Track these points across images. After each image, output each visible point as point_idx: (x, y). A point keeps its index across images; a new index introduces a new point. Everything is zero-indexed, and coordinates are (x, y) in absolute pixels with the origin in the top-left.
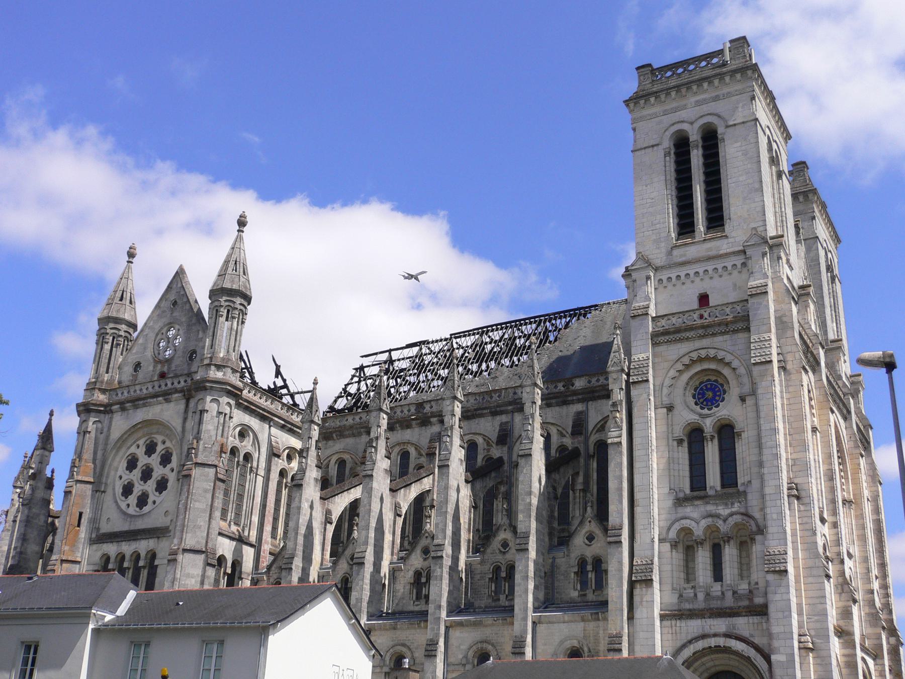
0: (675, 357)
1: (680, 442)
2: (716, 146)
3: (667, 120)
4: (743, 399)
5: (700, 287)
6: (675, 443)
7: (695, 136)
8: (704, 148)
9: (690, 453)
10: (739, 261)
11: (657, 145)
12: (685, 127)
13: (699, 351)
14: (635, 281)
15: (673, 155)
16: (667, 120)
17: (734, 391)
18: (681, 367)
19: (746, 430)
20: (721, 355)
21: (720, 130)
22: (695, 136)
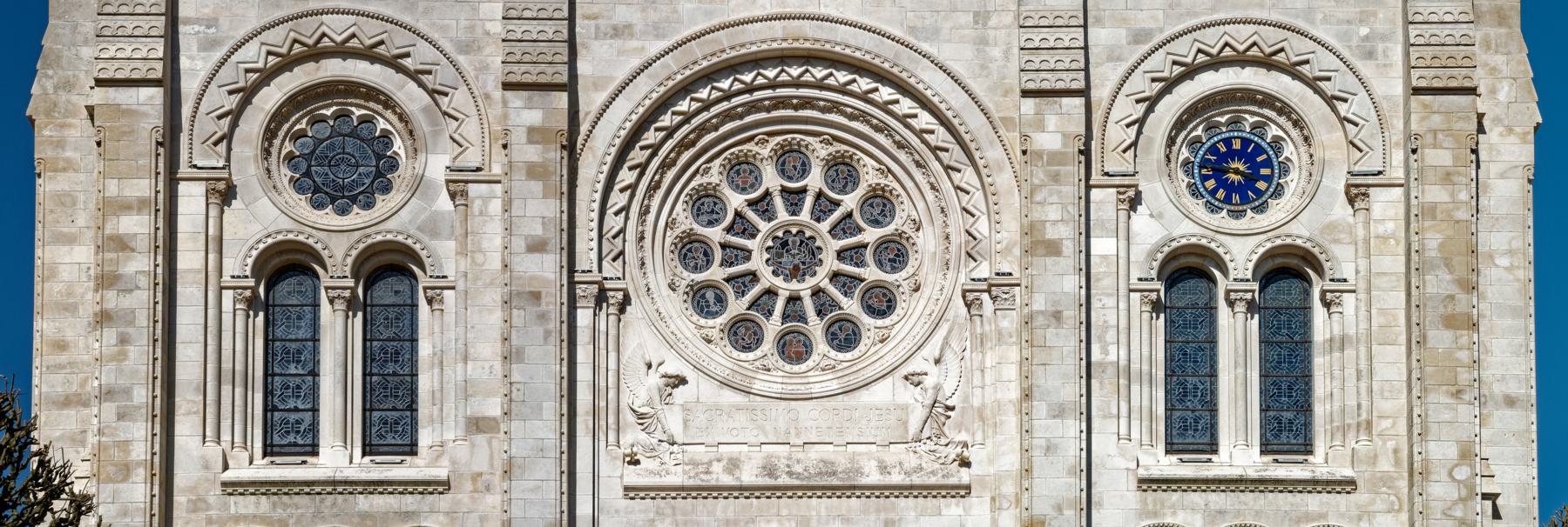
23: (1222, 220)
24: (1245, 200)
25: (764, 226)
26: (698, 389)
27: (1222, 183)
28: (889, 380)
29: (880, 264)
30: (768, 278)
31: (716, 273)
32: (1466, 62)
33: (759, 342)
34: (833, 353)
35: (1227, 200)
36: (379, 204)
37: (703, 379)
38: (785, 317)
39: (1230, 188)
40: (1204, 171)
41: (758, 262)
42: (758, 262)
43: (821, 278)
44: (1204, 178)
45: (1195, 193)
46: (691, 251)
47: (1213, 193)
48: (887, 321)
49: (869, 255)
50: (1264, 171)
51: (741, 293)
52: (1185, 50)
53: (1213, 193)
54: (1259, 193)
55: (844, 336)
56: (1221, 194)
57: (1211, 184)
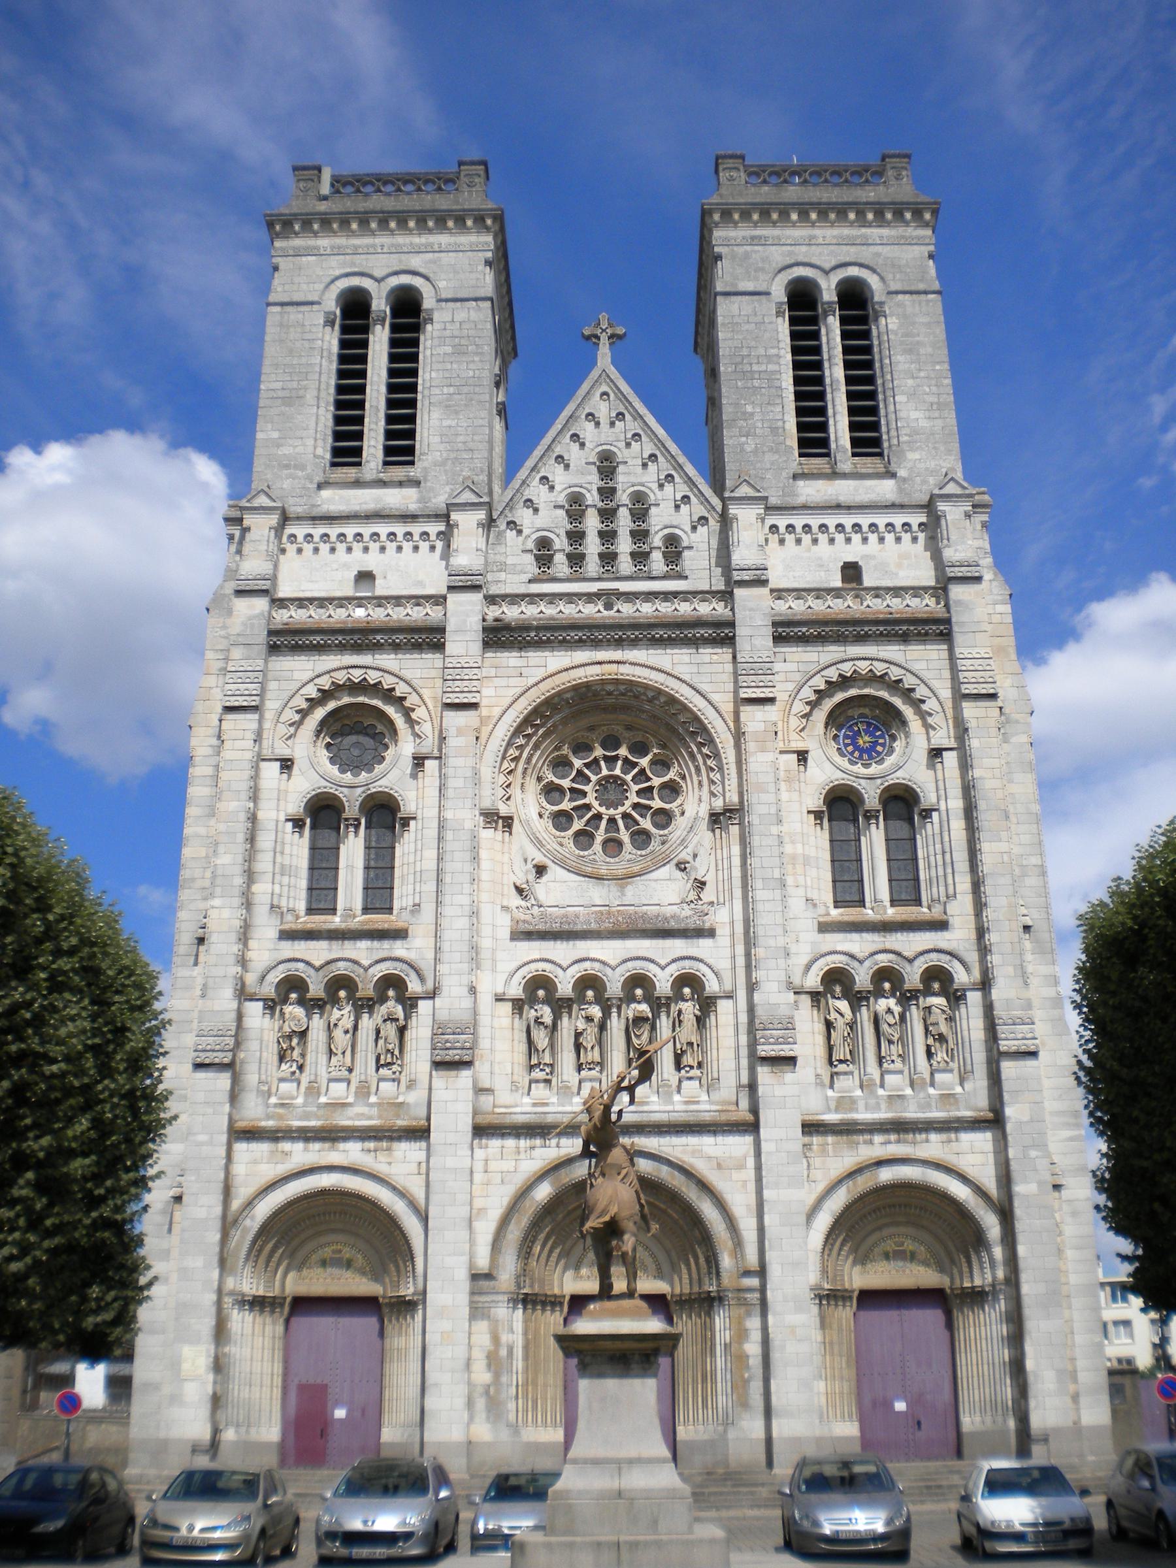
0: (310, 675)
1: (298, 824)
2: (417, 328)
3: (335, 266)
4: (419, 761)
5: (359, 560)
6: (290, 824)
7: (380, 304)
8: (394, 328)
9: (313, 848)
10: (434, 528)
11: (312, 303)
12: (367, 283)
13: (350, 671)
14: (246, 530)
15: (337, 327)
16: (335, 266)
17: (405, 747)
18: (314, 694)
19: (419, 817)
20: (388, 681)
21: (428, 303)
22: (380, 304)
23: (859, 769)
24: (871, 758)
25: (594, 778)
26: (555, 872)
27: (857, 748)
28: (668, 866)
29: (661, 799)
30: (597, 807)
31: (566, 805)
32: (991, 680)
33: (591, 846)
34: (635, 851)
35: (861, 758)
36: (376, 770)
37: (560, 870)
38: (607, 831)
39: (862, 751)
40: (847, 741)
41: (591, 799)
42: (591, 799)
43: (627, 807)
44: (846, 745)
45: (842, 755)
46: (551, 791)
47: (852, 754)
48: (666, 832)
49: (655, 791)
50: (881, 741)
51: (580, 817)
52: (833, 674)
53: (852, 754)
54: (879, 753)
55: (641, 838)
56: (856, 754)
57: (850, 748)
